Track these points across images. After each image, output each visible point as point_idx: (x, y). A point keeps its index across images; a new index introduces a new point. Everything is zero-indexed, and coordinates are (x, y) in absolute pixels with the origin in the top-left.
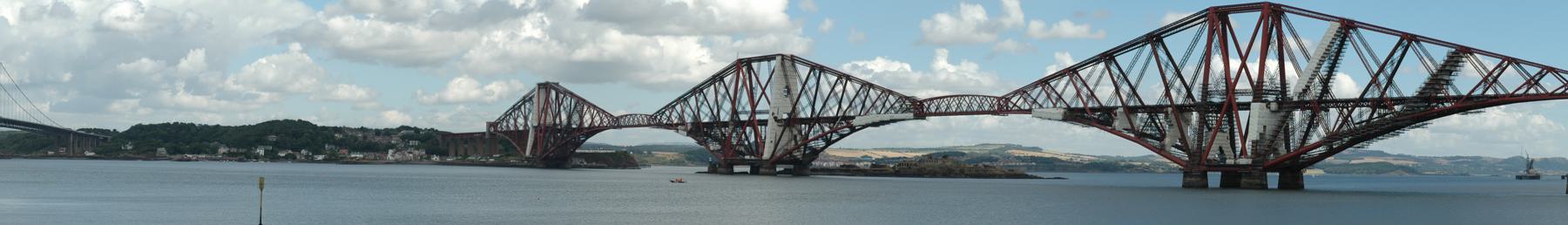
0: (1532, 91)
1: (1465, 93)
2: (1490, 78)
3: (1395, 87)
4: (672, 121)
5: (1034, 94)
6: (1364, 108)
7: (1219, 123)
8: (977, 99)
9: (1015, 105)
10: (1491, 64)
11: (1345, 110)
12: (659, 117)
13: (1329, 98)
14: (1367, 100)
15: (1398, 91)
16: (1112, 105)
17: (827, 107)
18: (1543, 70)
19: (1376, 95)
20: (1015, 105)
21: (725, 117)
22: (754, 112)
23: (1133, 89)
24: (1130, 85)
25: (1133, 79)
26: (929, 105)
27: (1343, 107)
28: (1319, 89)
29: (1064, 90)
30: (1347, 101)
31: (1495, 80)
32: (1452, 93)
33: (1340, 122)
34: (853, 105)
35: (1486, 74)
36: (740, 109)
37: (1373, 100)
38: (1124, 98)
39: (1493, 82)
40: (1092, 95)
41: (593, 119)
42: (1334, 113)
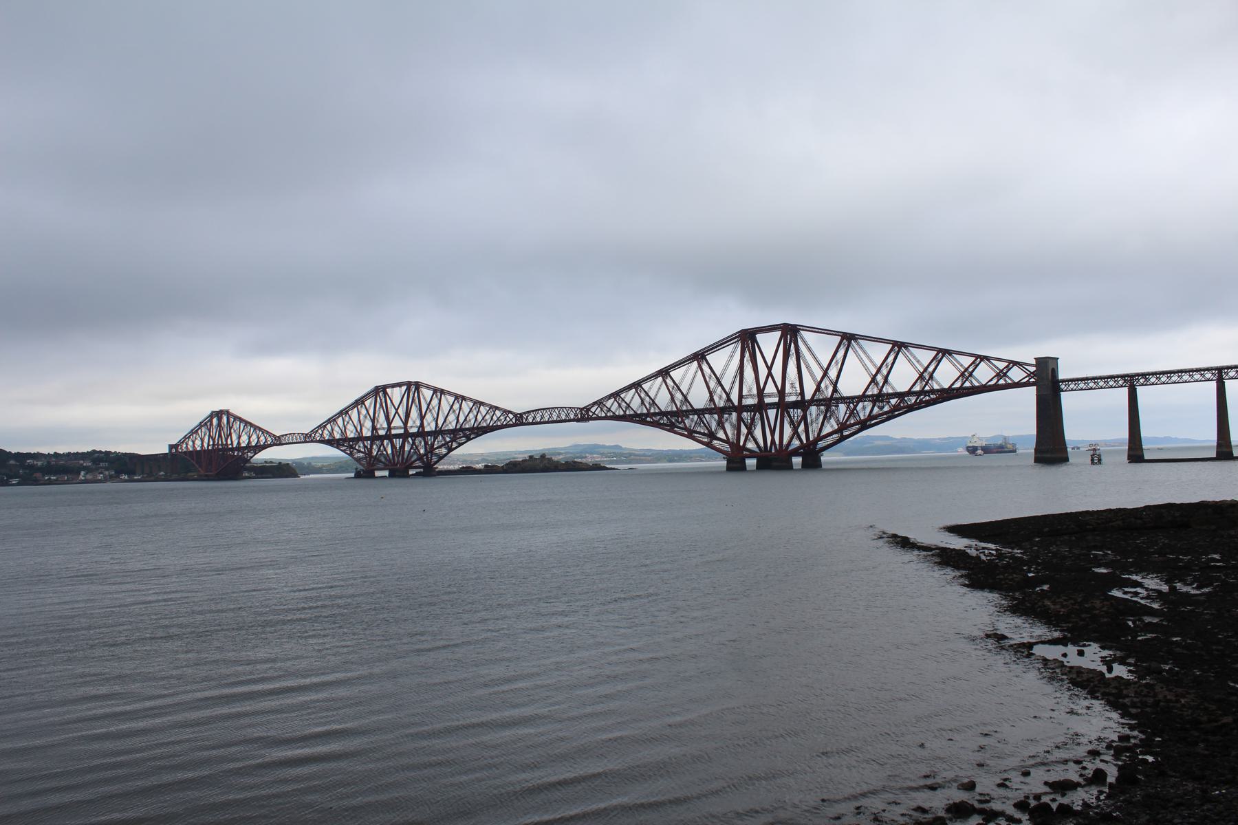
0: (1002, 382)
1: (946, 386)
2: (966, 373)
3: (890, 385)
4: (324, 438)
5: (609, 404)
6: (866, 403)
7: (753, 419)
8: (565, 410)
9: (594, 413)
10: (967, 360)
11: (851, 405)
12: (313, 435)
13: (838, 396)
14: (868, 396)
15: (893, 388)
16: (669, 410)
17: (448, 422)
18: (1009, 364)
19: (876, 391)
20: (594, 413)
21: (367, 432)
22: (389, 428)
23: (685, 397)
24: (682, 393)
25: (684, 389)
26: (527, 417)
27: (850, 403)
28: (831, 389)
29: (631, 400)
30: (852, 398)
31: (971, 374)
32: (936, 387)
33: (847, 415)
34: (468, 419)
35: (963, 370)
36: (378, 426)
37: (872, 396)
38: (678, 404)
39: (969, 376)
40: (653, 403)
41: (259, 438)
42: (842, 407)
